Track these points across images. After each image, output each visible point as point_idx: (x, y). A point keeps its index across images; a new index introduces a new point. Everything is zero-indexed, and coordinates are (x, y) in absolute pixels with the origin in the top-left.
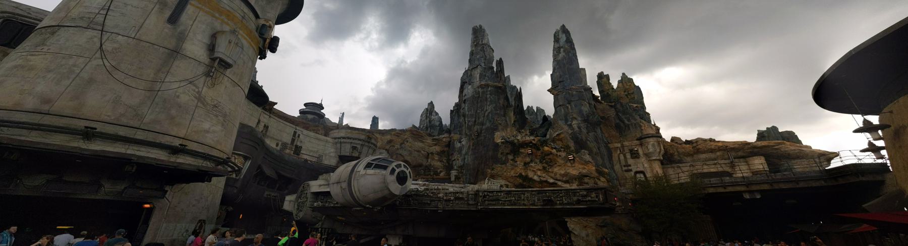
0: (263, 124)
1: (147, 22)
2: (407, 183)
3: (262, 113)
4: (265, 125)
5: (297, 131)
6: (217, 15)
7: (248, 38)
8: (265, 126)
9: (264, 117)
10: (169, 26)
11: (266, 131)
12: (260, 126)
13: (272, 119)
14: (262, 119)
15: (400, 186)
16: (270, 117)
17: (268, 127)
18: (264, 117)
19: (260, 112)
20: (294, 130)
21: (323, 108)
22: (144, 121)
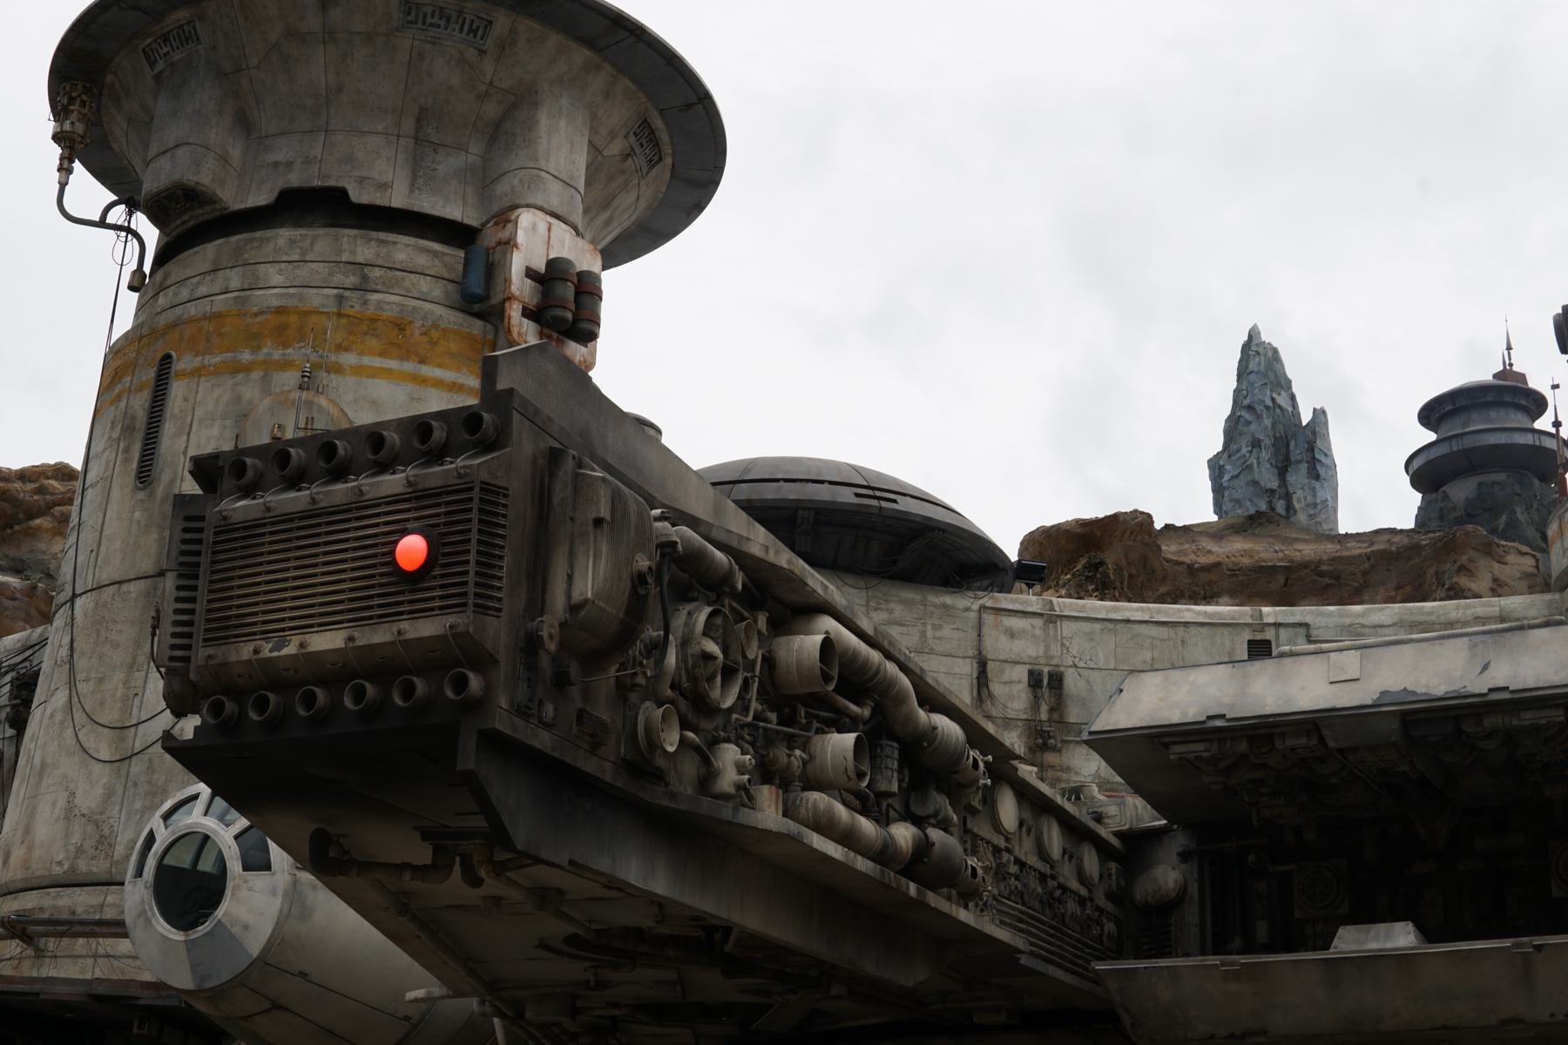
0: (1021, 673)
1: (108, 513)
2: (220, 912)
3: (989, 618)
4: (1031, 673)
5: (1269, 634)
6: (246, 356)
7: (393, 364)
8: (1035, 680)
9: (1012, 634)
10: (141, 495)
11: (1058, 706)
12: (997, 688)
13: (1067, 628)
14: (998, 645)
15: (177, 936)
16: (1051, 618)
17: (1057, 680)
18: (1012, 634)
19: (973, 615)
20: (1247, 635)
21: (1537, 404)
22: (115, 859)
